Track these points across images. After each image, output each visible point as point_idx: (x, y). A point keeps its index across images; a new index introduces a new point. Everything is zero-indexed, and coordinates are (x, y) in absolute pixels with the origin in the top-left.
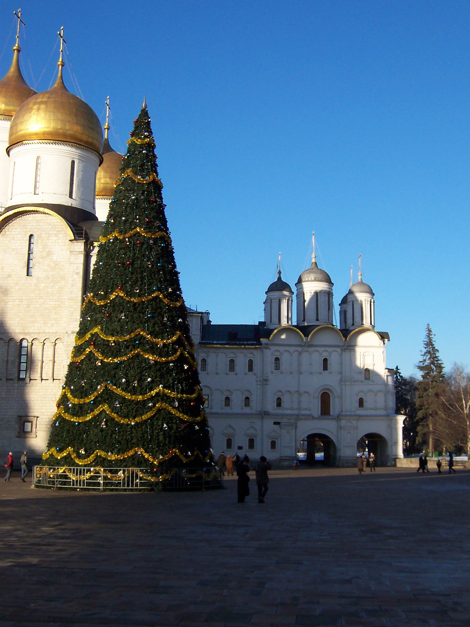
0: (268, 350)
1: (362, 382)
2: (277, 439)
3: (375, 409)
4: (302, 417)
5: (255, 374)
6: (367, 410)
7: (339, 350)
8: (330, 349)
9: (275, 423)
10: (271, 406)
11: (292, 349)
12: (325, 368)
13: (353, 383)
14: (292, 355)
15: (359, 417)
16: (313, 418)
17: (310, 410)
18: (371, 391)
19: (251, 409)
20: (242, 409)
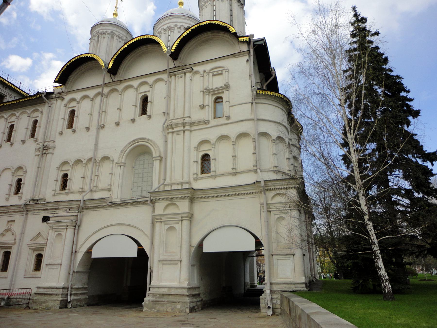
0: (59, 101)
1: (206, 122)
2: (42, 249)
3: (235, 173)
4: (89, 204)
5: (36, 140)
6: (215, 177)
7: (165, 76)
8: (150, 80)
9: (46, 219)
10: (49, 191)
11: (91, 93)
12: (144, 111)
13: (187, 127)
14: (92, 100)
15: (193, 195)
16: (112, 205)
17: (110, 190)
18: (224, 137)
19: (20, 198)
20: (7, 199)
